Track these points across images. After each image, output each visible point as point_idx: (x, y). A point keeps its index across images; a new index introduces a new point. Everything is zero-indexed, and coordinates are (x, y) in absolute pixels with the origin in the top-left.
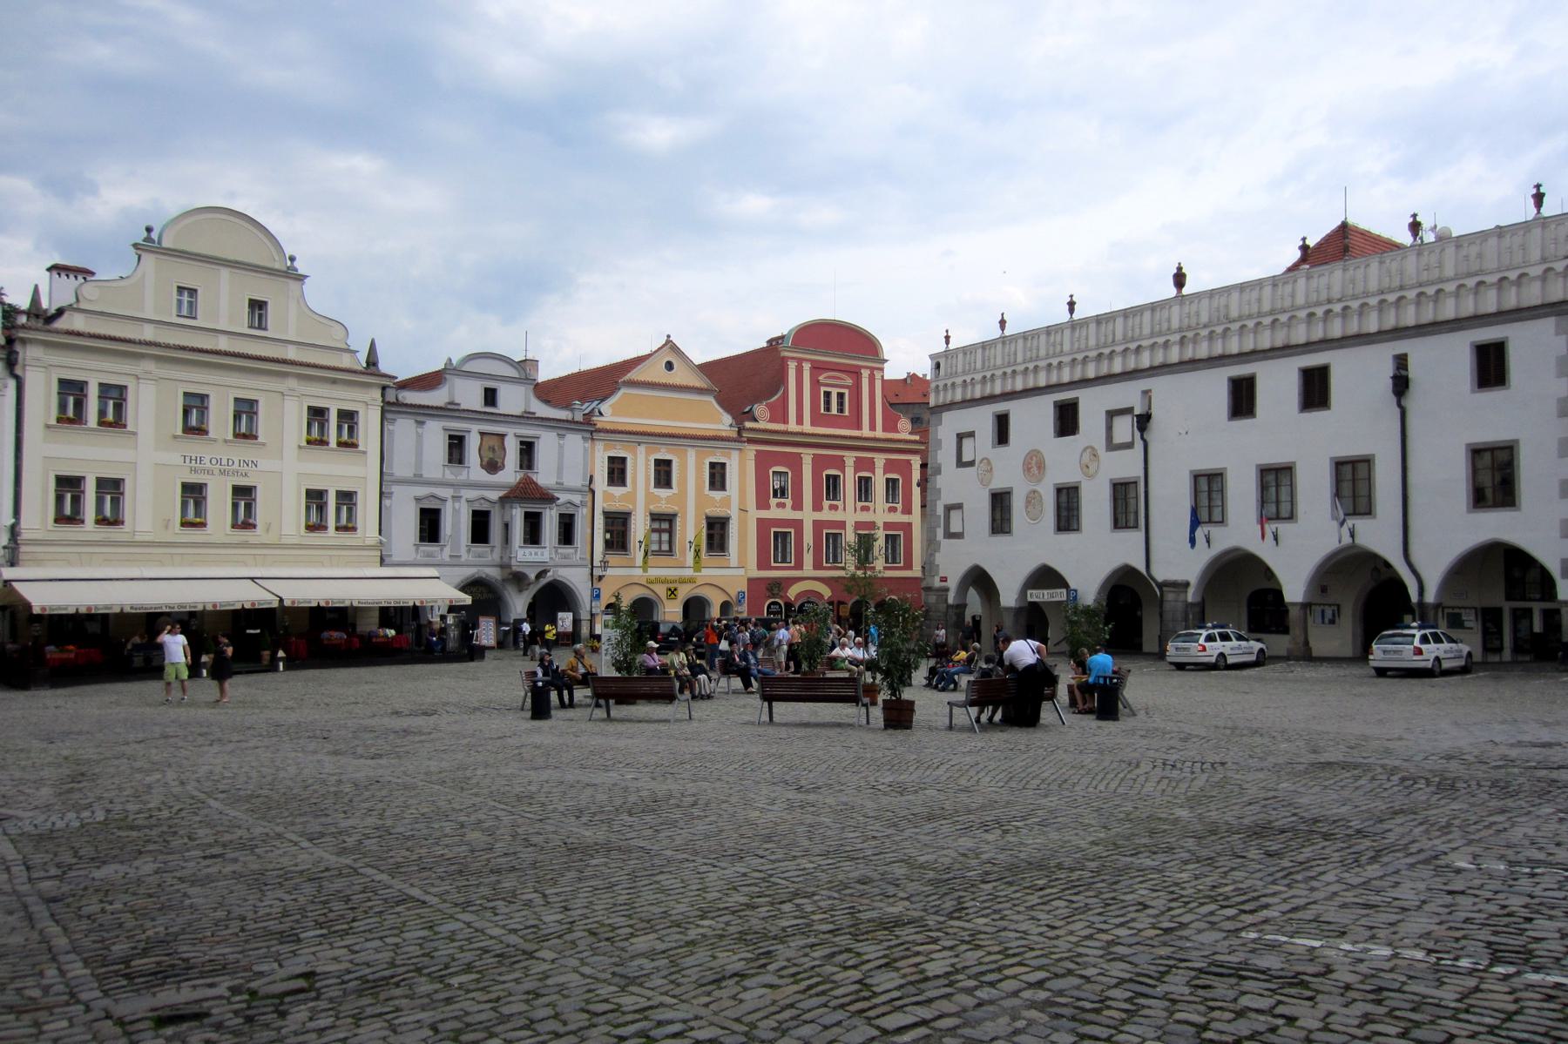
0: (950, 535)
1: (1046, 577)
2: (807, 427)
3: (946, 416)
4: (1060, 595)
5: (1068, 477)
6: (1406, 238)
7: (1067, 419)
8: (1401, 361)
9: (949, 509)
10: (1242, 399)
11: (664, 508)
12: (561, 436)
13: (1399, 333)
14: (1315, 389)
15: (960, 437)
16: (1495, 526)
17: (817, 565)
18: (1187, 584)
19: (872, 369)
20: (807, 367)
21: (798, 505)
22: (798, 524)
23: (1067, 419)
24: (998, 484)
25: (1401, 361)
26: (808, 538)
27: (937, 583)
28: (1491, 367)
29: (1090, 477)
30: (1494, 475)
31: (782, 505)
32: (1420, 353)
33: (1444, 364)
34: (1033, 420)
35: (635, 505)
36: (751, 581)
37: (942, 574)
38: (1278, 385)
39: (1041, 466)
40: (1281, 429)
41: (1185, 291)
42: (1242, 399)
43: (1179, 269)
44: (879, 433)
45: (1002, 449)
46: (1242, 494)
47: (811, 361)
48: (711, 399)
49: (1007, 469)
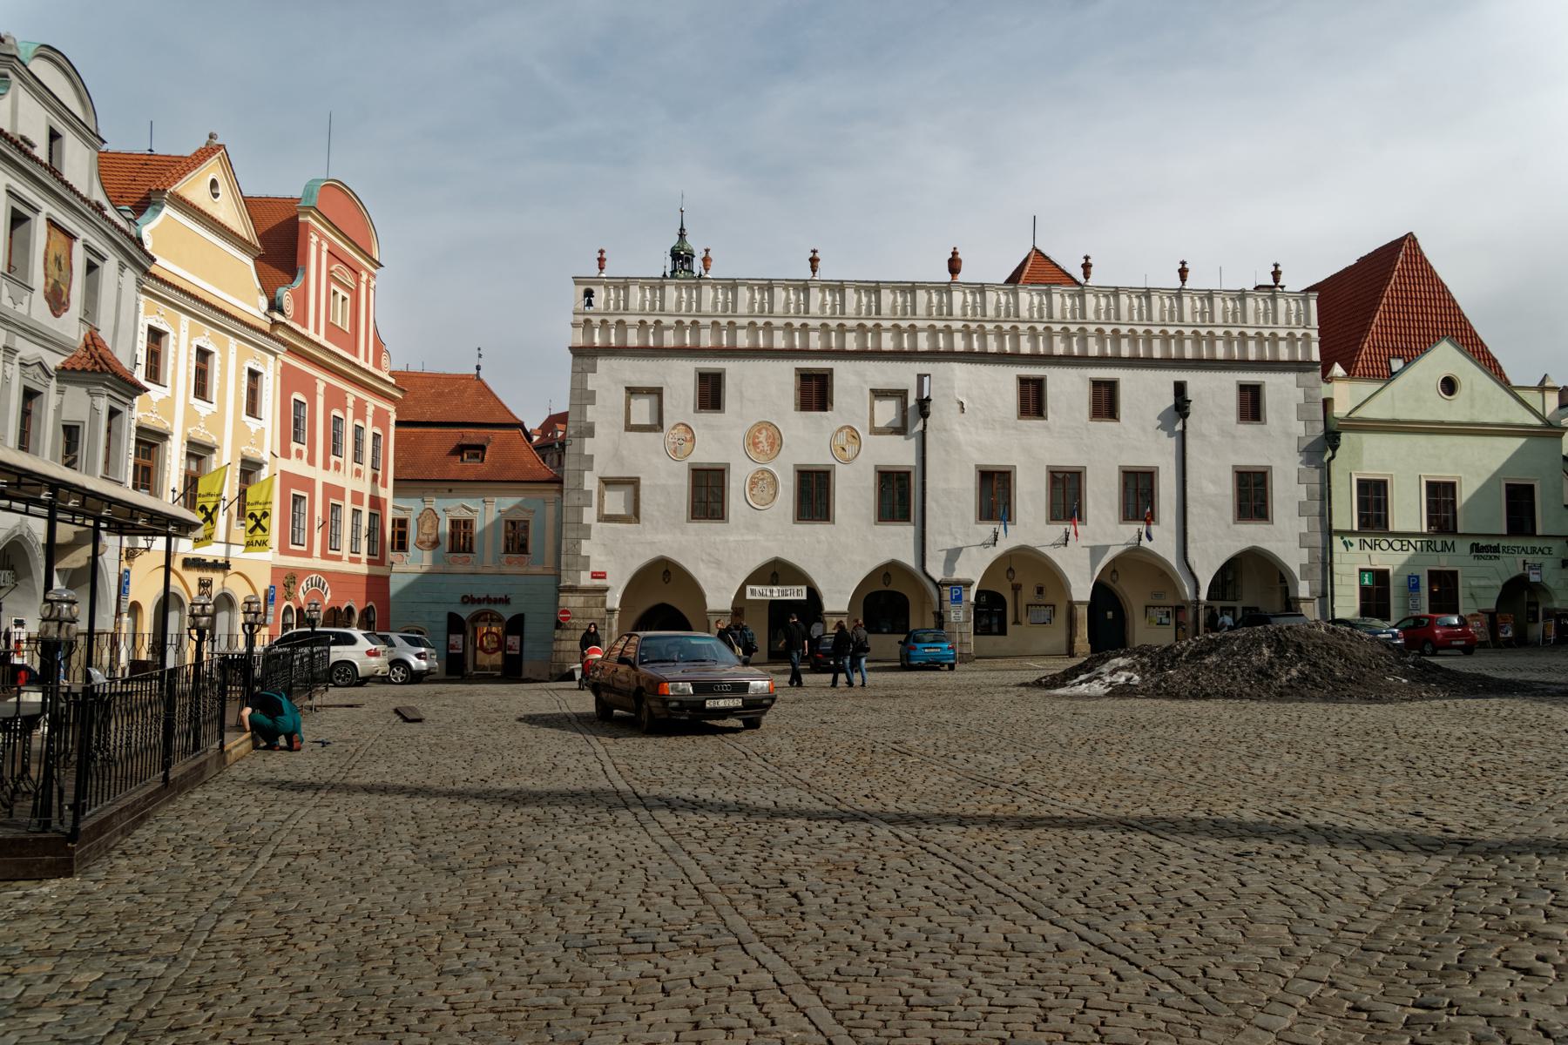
0: (606, 519)
1: (777, 571)
2: (320, 339)
3: (602, 363)
4: (798, 593)
5: (817, 457)
6: (1078, 275)
7: (815, 393)
8: (1180, 388)
9: (608, 483)
10: (1033, 400)
11: (203, 435)
12: (122, 267)
13: (1180, 363)
14: (1105, 402)
15: (632, 391)
16: (1252, 535)
17: (324, 556)
18: (968, 584)
19: (370, 274)
20: (325, 247)
21: (311, 461)
22: (308, 483)
23: (815, 393)
24: (706, 454)
25: (1180, 388)
26: (319, 512)
27: (585, 580)
28: (1251, 405)
29: (848, 461)
30: (1252, 493)
31: (299, 454)
32: (1196, 382)
33: (1215, 393)
34: (761, 389)
35: (171, 419)
36: (276, 570)
37: (594, 568)
38: (1068, 389)
39: (776, 442)
40: (1067, 435)
41: (960, 278)
42: (1033, 400)
43: (954, 254)
44: (370, 367)
45: (710, 417)
46: (1030, 495)
47: (330, 243)
48: (250, 262)
49: (718, 440)
